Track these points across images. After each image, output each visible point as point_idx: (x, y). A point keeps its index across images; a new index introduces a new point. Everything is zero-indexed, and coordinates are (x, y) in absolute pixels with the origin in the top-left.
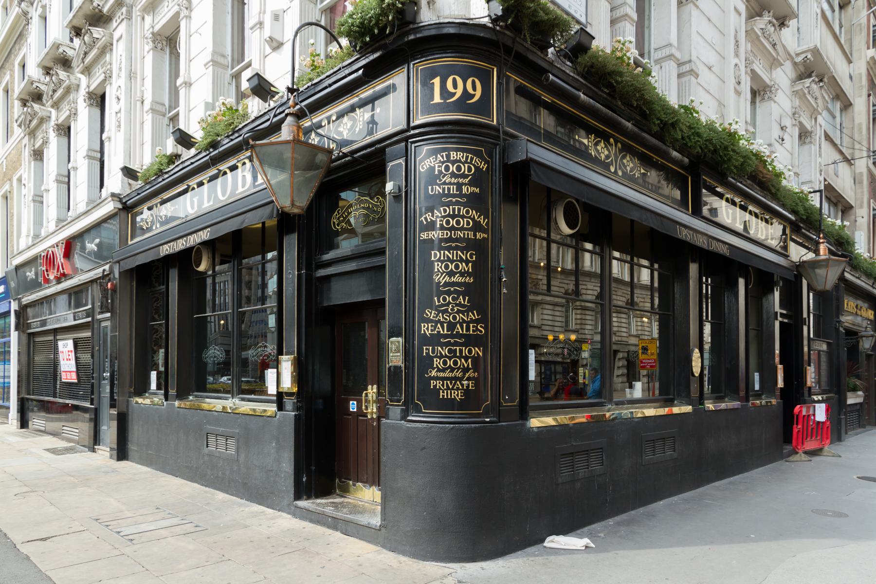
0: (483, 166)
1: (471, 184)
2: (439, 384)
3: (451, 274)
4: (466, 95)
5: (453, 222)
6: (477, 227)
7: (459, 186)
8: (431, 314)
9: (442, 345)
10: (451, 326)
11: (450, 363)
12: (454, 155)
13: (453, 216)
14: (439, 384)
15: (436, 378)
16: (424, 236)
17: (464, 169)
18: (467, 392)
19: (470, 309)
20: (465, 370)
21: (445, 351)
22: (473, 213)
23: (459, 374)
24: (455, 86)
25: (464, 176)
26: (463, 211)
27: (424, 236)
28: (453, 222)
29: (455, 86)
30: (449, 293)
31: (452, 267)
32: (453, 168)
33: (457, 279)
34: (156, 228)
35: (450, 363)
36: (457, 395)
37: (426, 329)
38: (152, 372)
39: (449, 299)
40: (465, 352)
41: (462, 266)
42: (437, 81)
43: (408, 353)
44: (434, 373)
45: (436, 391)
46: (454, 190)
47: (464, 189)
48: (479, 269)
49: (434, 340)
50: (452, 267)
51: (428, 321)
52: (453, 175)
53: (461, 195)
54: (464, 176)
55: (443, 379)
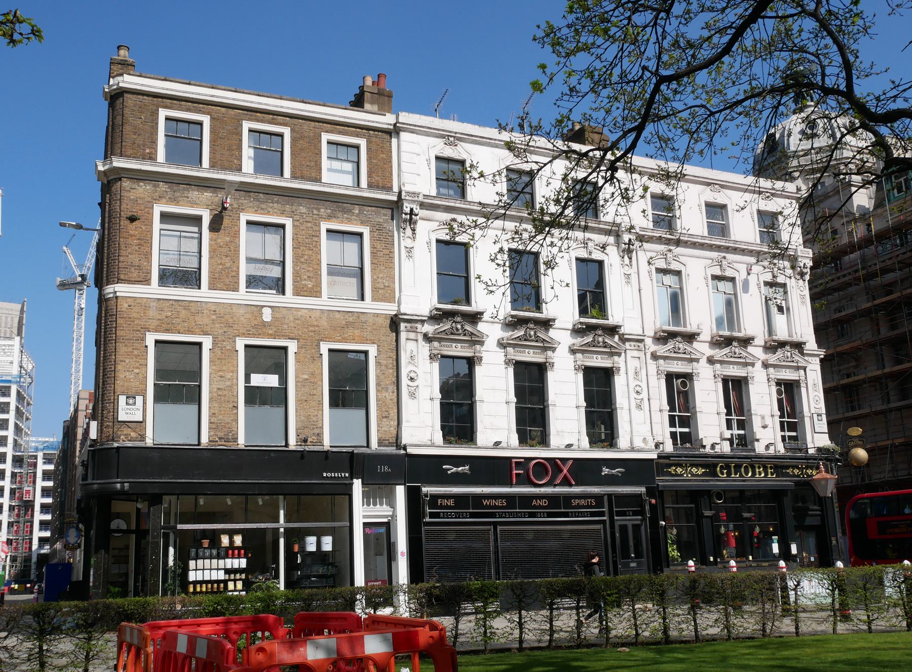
34: (687, 476)
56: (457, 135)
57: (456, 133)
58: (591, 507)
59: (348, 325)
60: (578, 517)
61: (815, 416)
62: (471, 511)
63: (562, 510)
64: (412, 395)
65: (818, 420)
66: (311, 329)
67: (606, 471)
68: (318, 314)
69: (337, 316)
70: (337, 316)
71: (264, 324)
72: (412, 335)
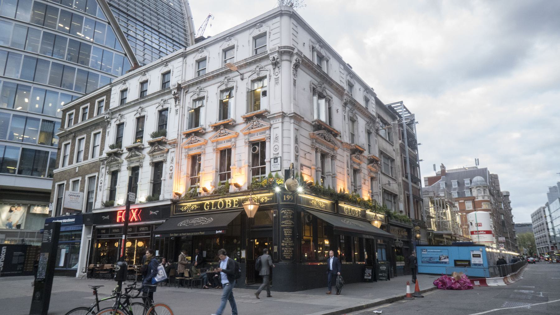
0: (293, 212)
1: (291, 216)
2: (285, 256)
3: (288, 233)
4: (290, 199)
5: (288, 223)
6: (292, 224)
7: (289, 216)
8: (283, 241)
9: (286, 248)
10: (288, 244)
11: (288, 251)
12: (288, 210)
13: (288, 222)
14: (285, 256)
15: (285, 254)
16: (282, 226)
17: (290, 213)
18: (291, 257)
19: (291, 240)
20: (290, 253)
21: (287, 249)
22: (292, 221)
23: (289, 253)
24: (288, 197)
25: (290, 214)
26: (290, 221)
27: (282, 226)
28: (288, 223)
29: (288, 197)
30: (287, 237)
31: (288, 232)
32: (288, 213)
33: (289, 234)
34: (189, 211)
35: (288, 251)
36: (289, 258)
37: (283, 244)
38: (204, 252)
39: (287, 238)
40: (291, 249)
41: (290, 232)
42: (285, 196)
43: (278, 249)
44: (284, 253)
45: (285, 257)
46: (288, 217)
47: (290, 217)
48: (293, 233)
49: (285, 247)
50: (288, 232)
51: (283, 243)
52: (288, 214)
53: (290, 218)
54: (290, 214)
55: (286, 254)
56: (125, 79)
57: (124, 78)
58: (146, 231)
59: (93, 167)
60: (141, 236)
61: (273, 160)
62: (109, 234)
63: (136, 233)
64: (101, 190)
65: (274, 162)
66: (85, 171)
67: (151, 213)
68: (87, 166)
69: (91, 164)
70: (91, 164)
71: (77, 173)
72: (103, 166)
